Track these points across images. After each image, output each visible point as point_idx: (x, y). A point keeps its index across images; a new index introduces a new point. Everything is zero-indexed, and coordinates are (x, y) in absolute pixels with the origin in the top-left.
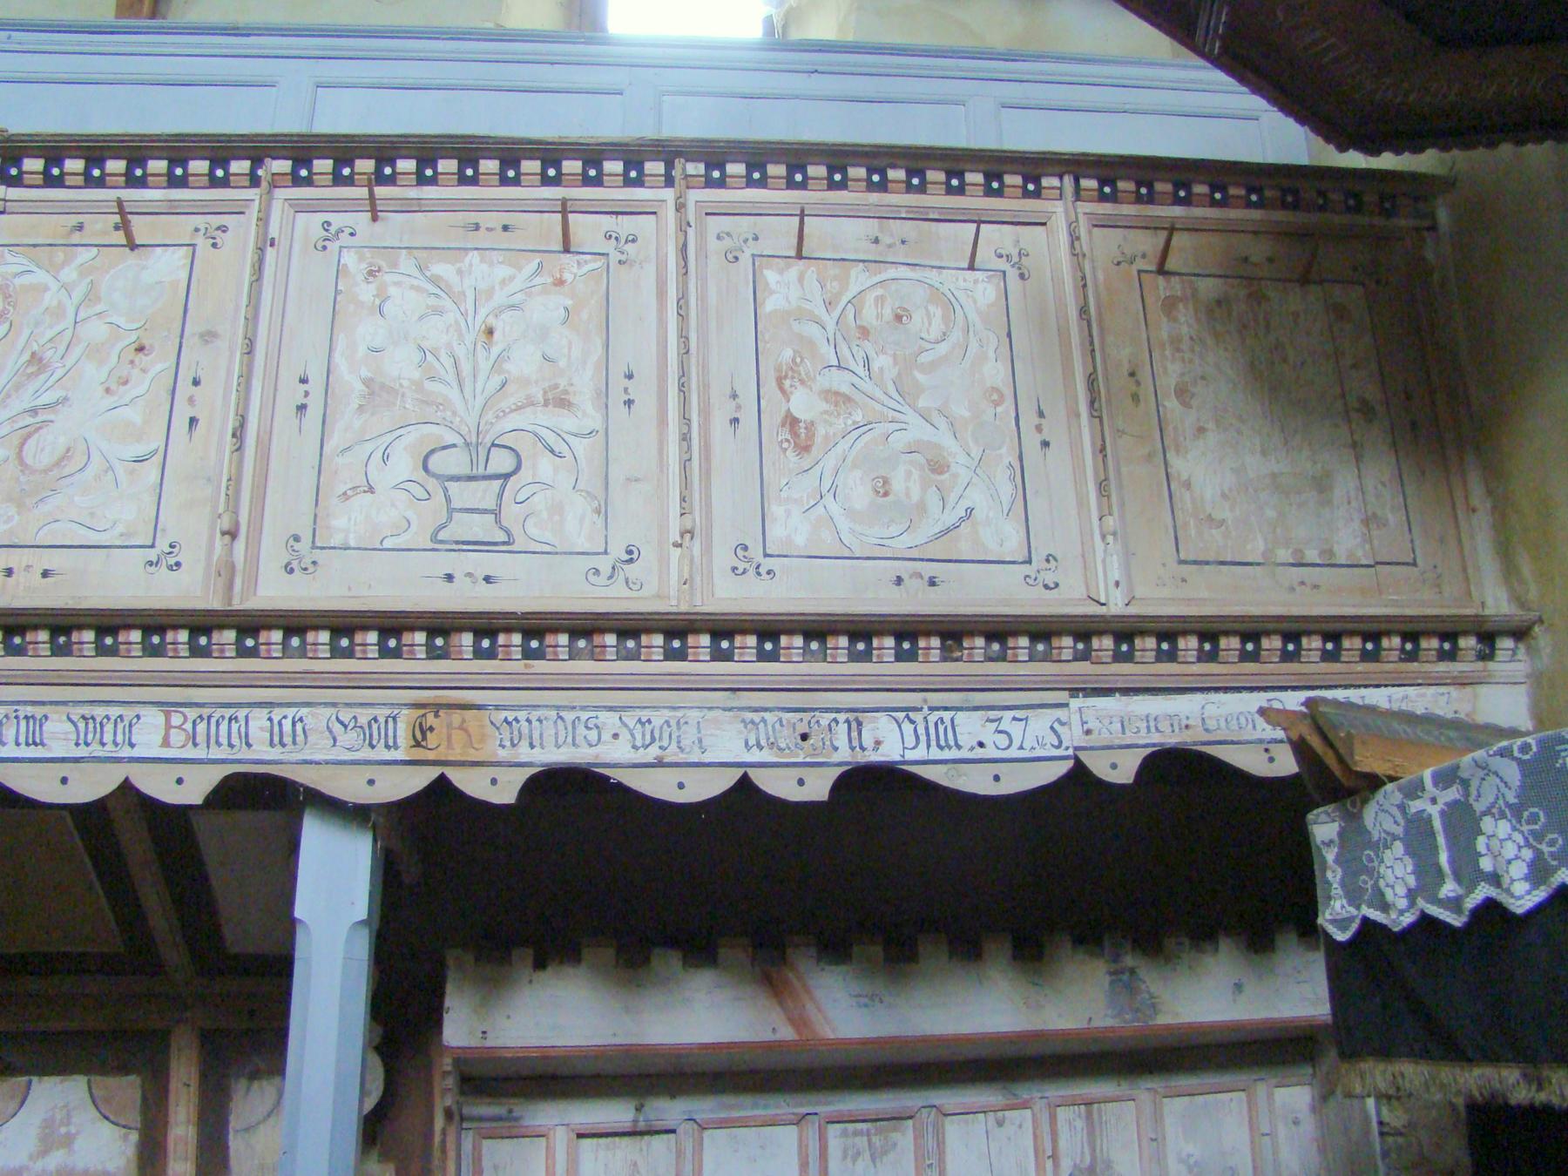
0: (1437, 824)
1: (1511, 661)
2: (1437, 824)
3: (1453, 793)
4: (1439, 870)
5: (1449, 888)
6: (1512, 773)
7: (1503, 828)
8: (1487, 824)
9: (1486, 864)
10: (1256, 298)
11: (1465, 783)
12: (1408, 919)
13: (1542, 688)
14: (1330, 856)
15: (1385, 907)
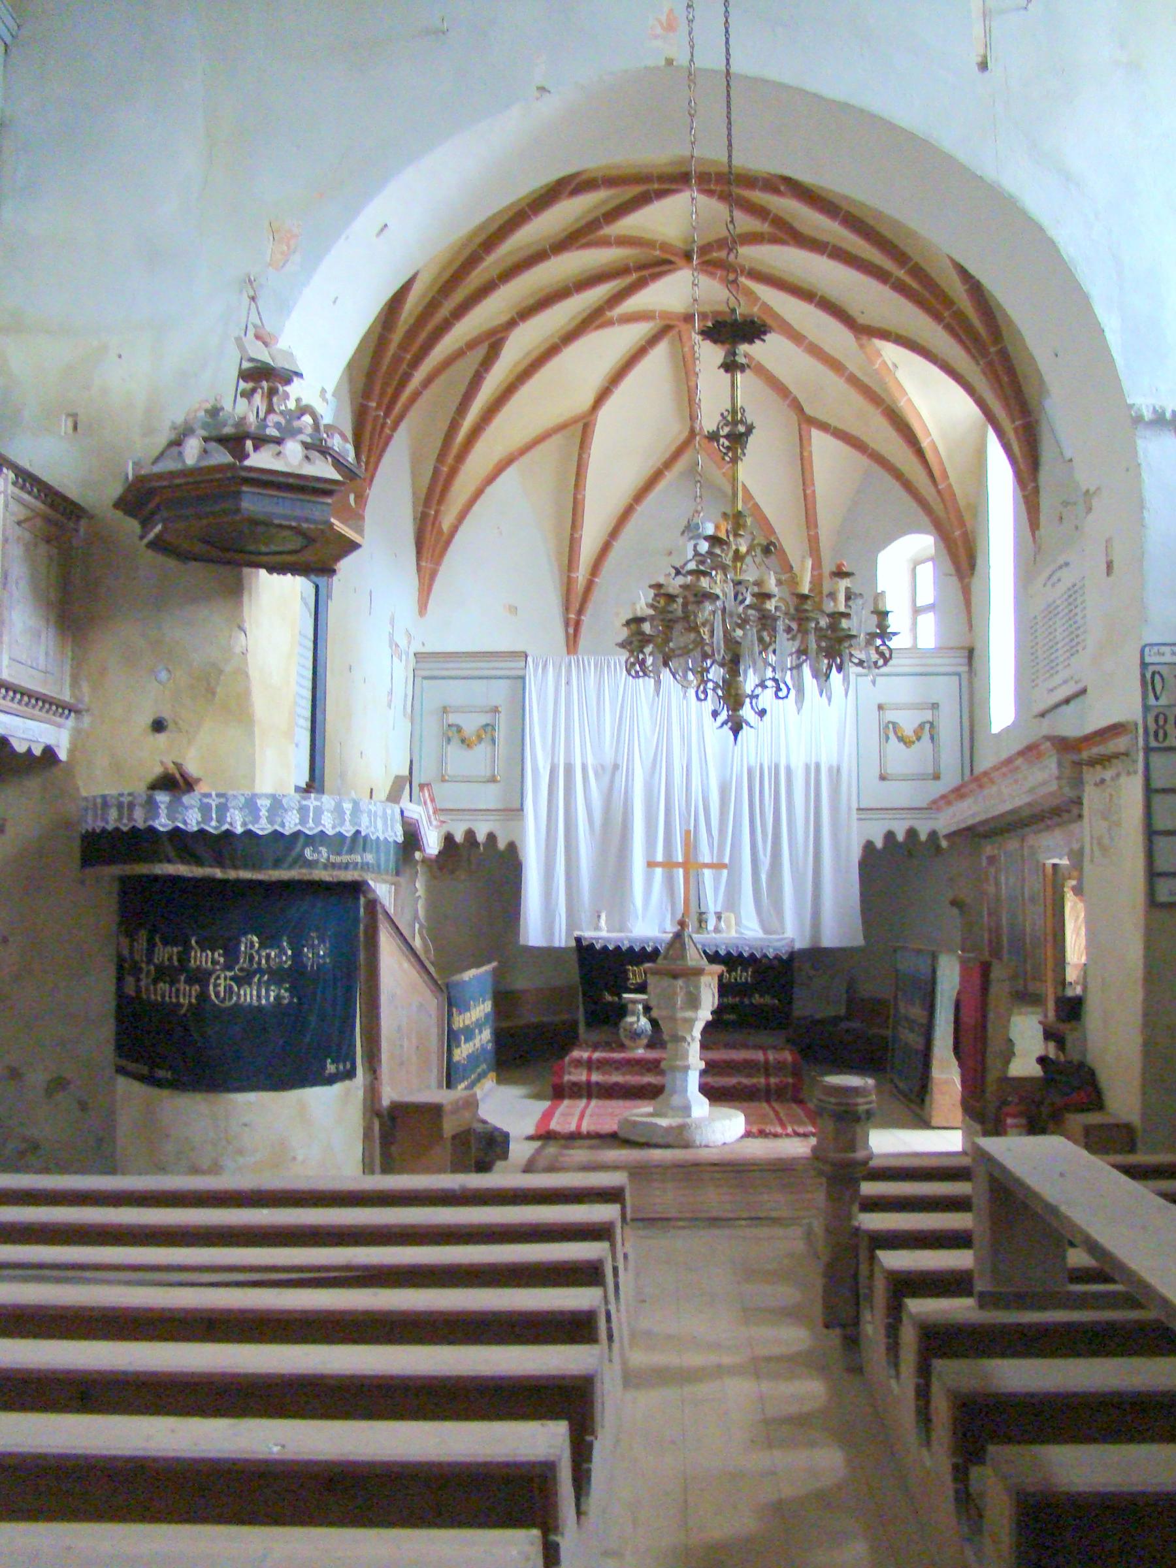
0: (214, 807)
1: (71, 722)
2: (214, 807)
3: (222, 800)
4: (211, 819)
5: (214, 823)
6: (243, 800)
7: (237, 812)
8: (232, 810)
9: (229, 820)
10: (36, 545)
11: (227, 800)
12: (195, 829)
13: (77, 734)
14: (163, 806)
15: (185, 823)
